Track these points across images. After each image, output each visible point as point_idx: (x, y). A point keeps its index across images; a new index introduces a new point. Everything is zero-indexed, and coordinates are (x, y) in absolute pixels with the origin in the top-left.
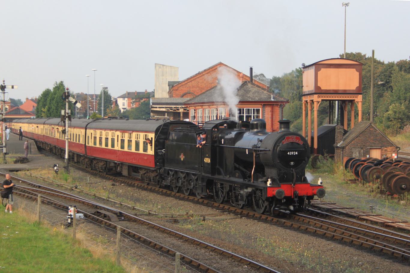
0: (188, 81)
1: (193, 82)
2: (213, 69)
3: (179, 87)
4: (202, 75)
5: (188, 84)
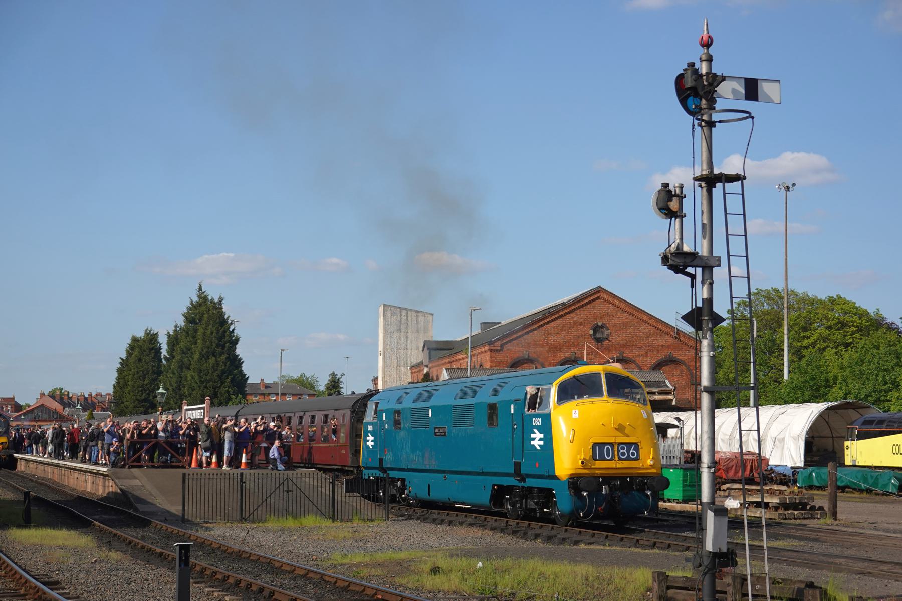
1: (535, 332)
2: (582, 303)
3: (505, 344)
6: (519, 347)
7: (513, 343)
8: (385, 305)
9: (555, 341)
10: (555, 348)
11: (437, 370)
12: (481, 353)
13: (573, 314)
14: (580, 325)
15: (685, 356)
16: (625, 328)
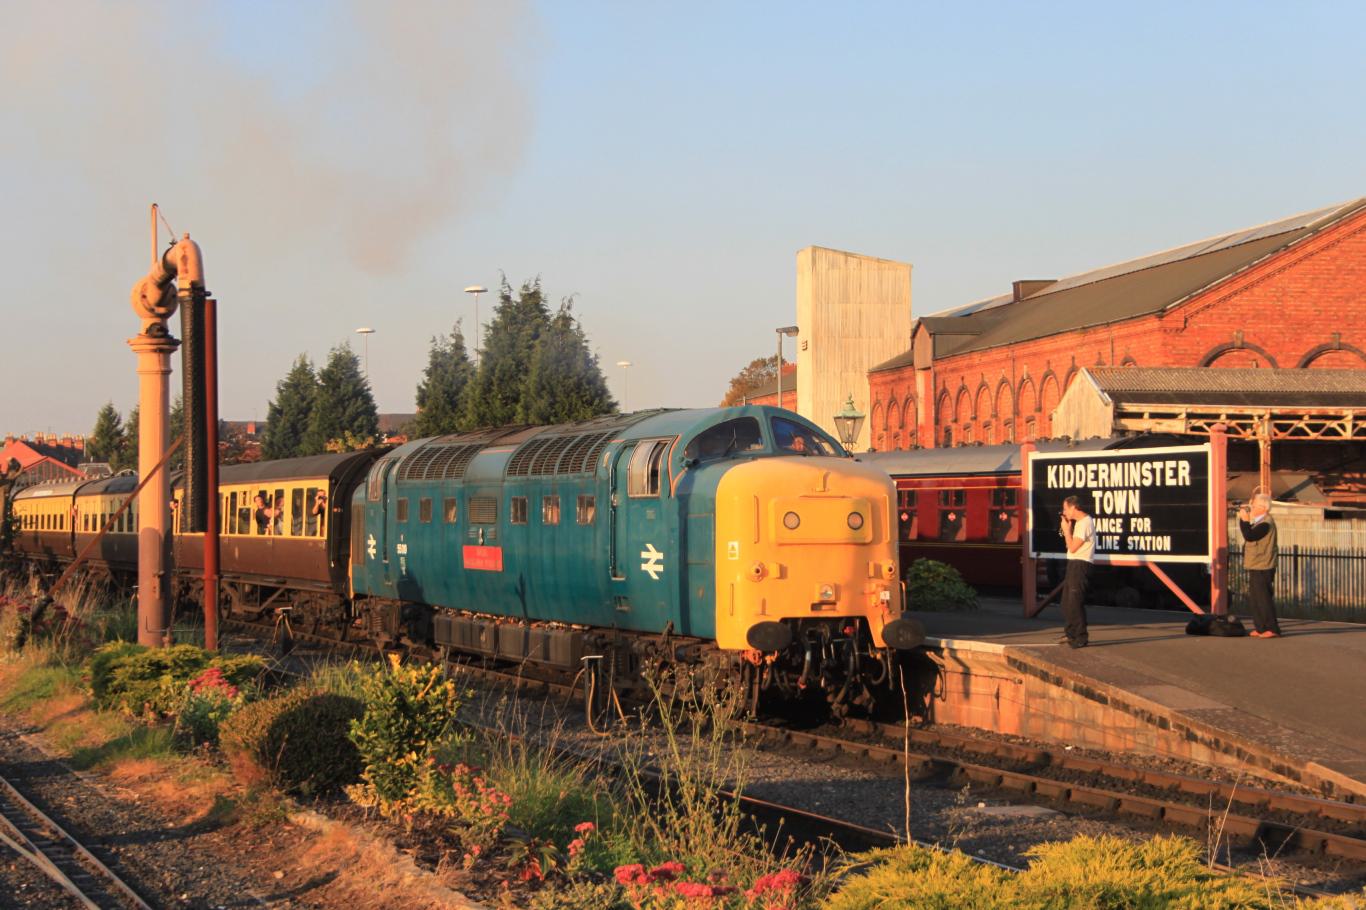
0: (1236, 287)
1: (1257, 290)
4: (1300, 254)
5: (1235, 299)
6: (1223, 323)
7: (1211, 315)
8: (815, 249)
9: (1297, 310)
10: (1298, 324)
11: (963, 378)
12: (1129, 336)
13: (1334, 252)
14: (1348, 274)
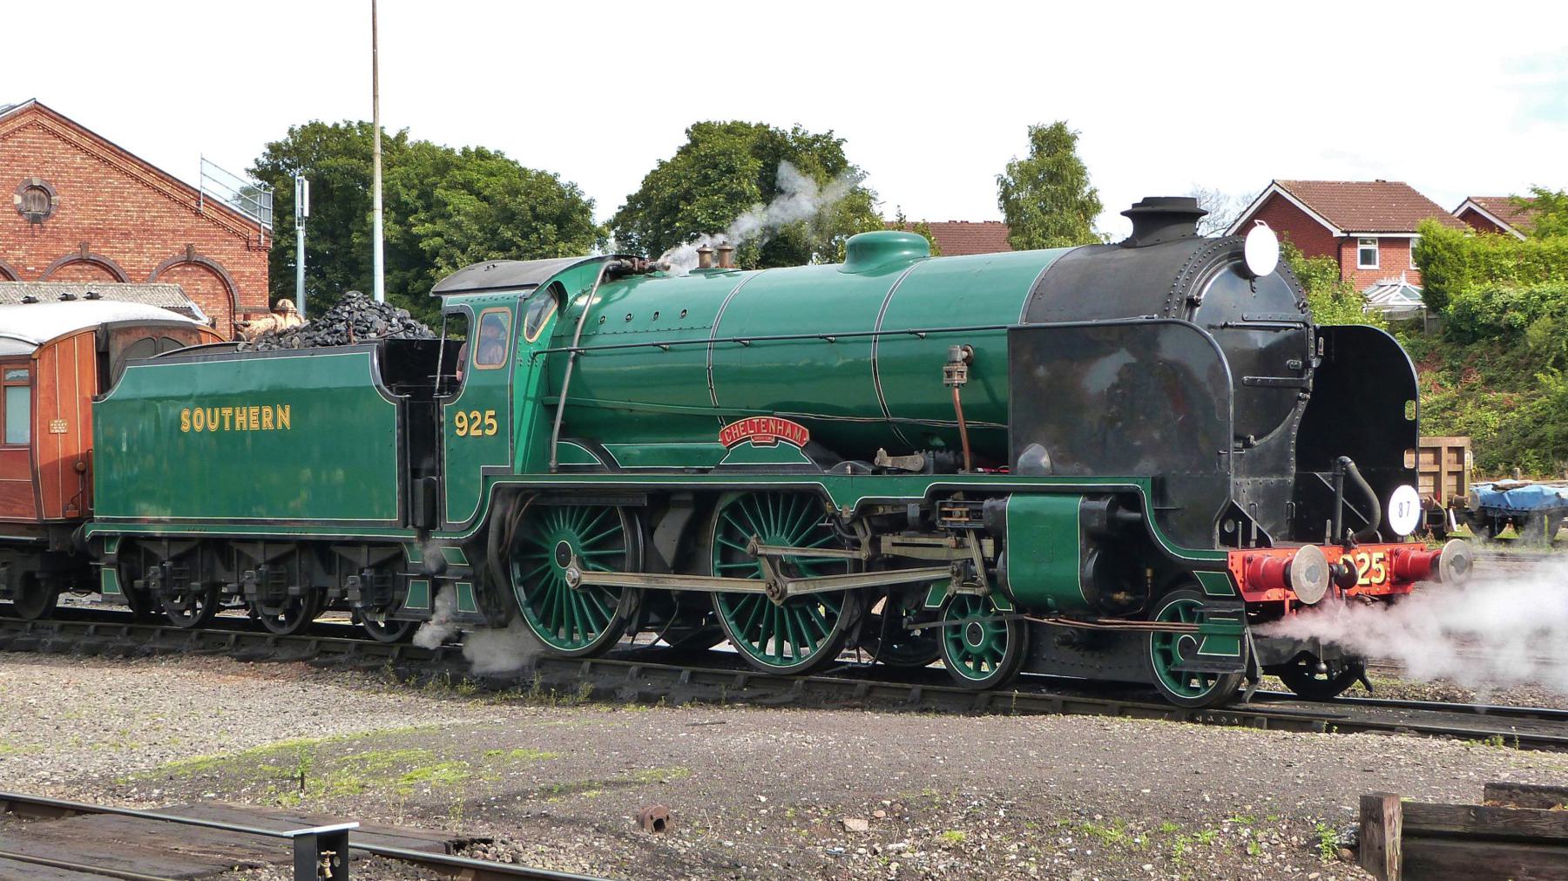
15: (220, 254)
16: (93, 192)
